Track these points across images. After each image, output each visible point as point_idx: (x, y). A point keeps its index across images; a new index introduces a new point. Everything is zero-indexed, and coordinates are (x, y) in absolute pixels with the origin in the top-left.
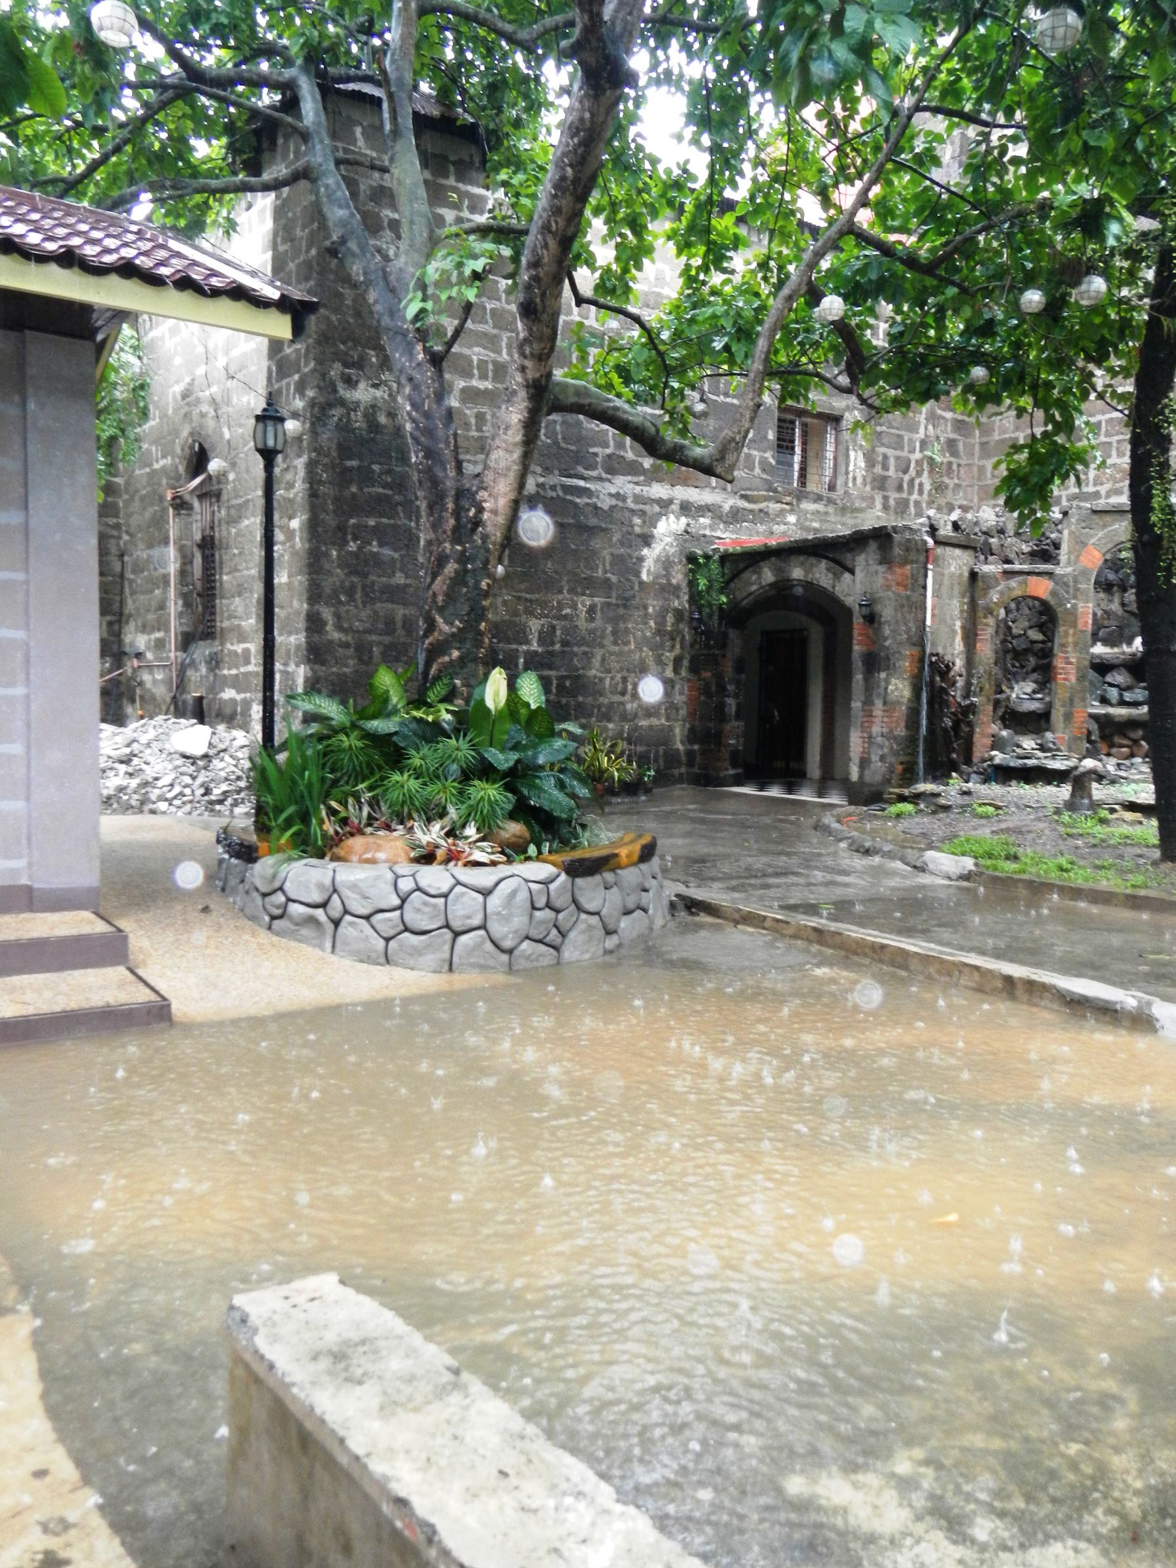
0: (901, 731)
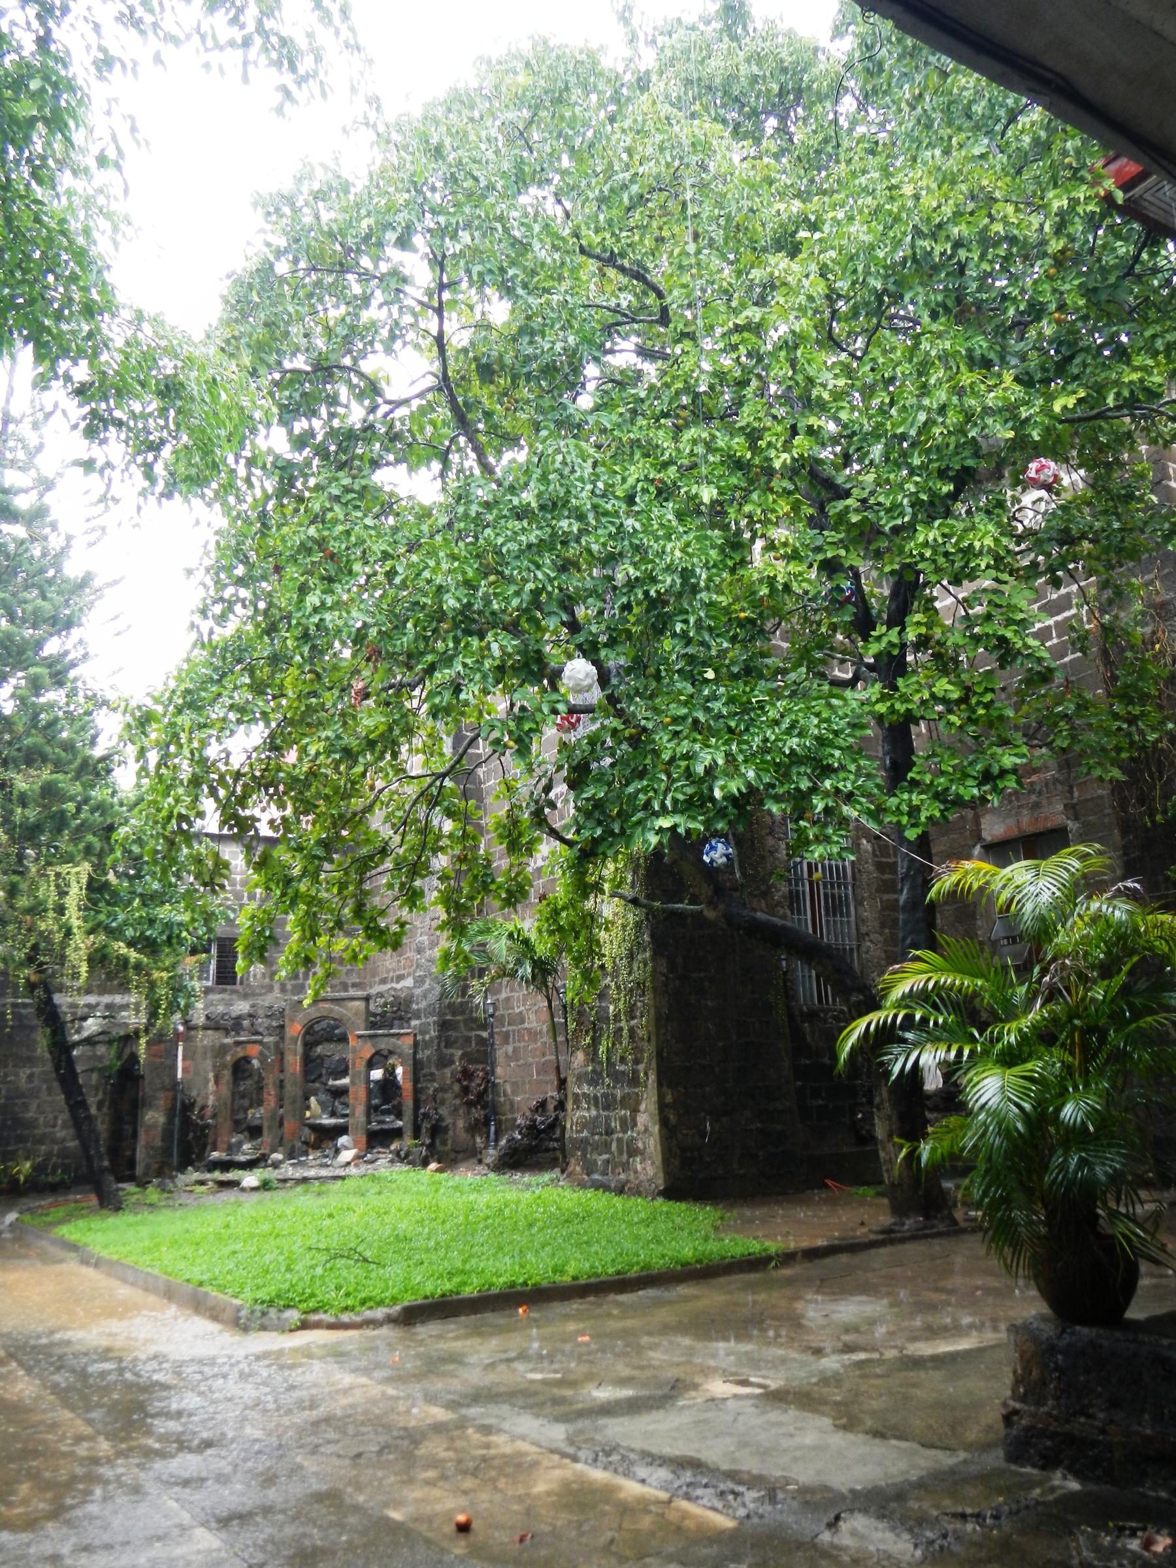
0: (158, 1143)
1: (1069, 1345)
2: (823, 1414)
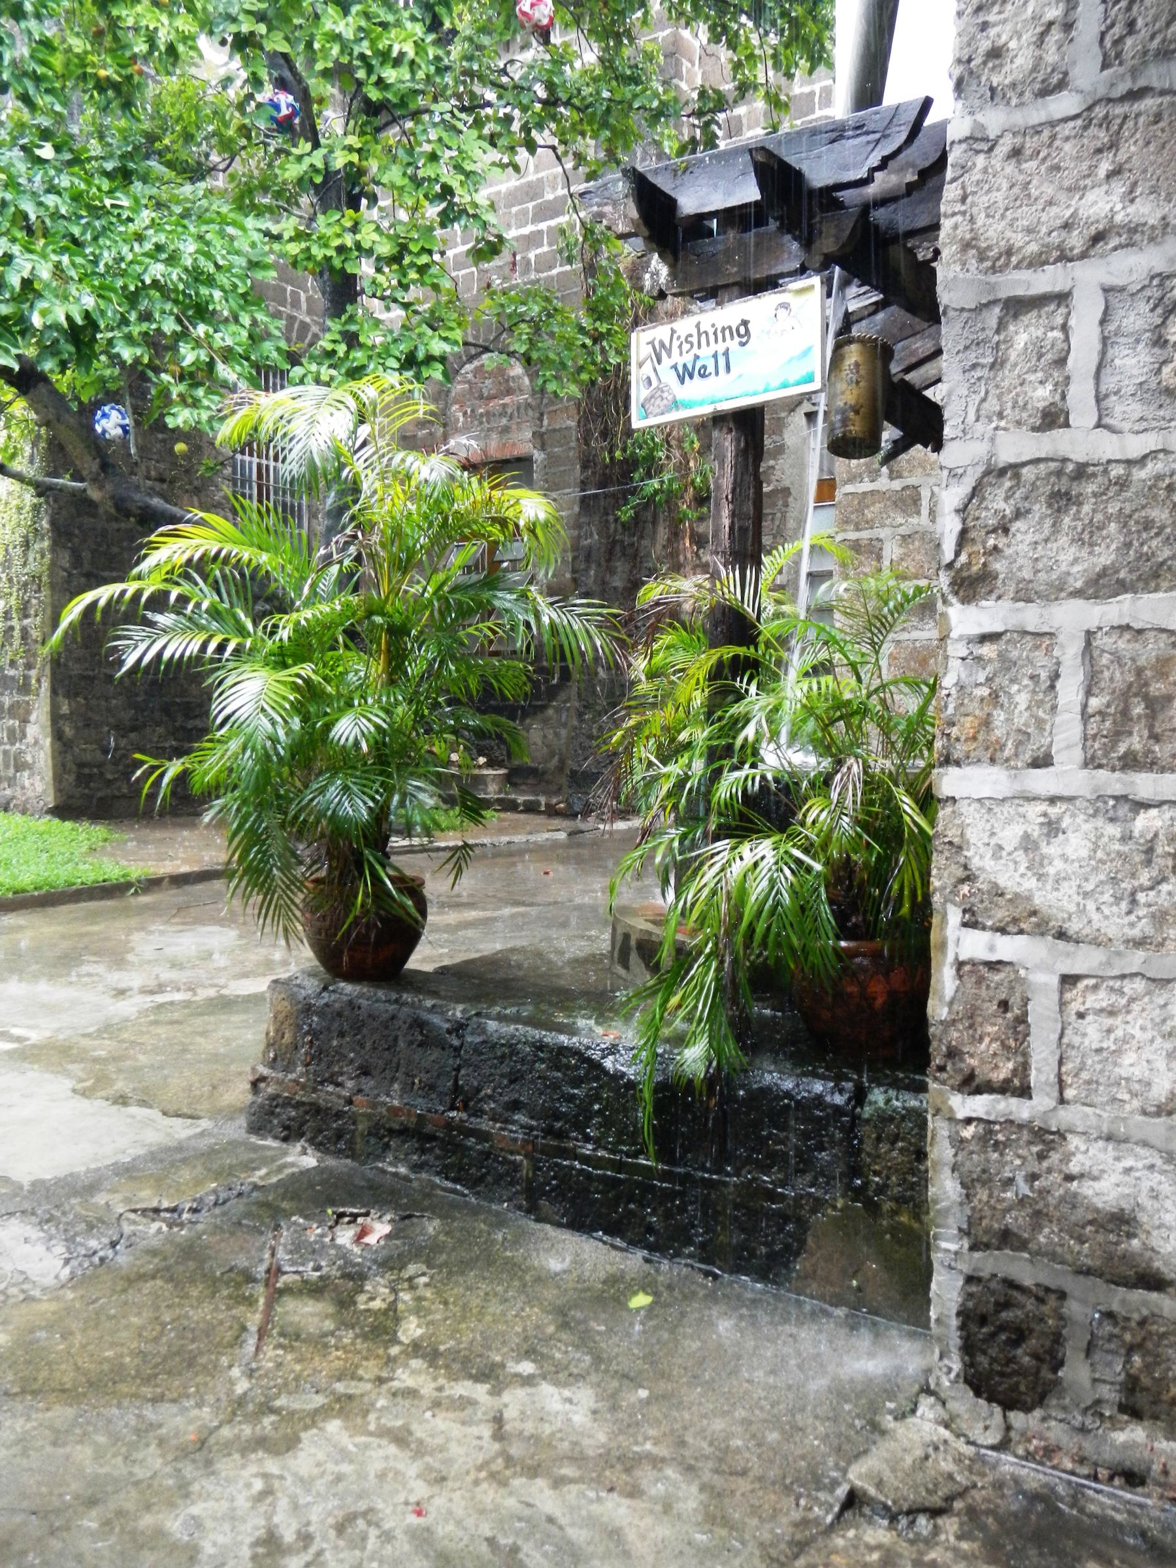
1: (327, 1005)
2: (68, 1074)
